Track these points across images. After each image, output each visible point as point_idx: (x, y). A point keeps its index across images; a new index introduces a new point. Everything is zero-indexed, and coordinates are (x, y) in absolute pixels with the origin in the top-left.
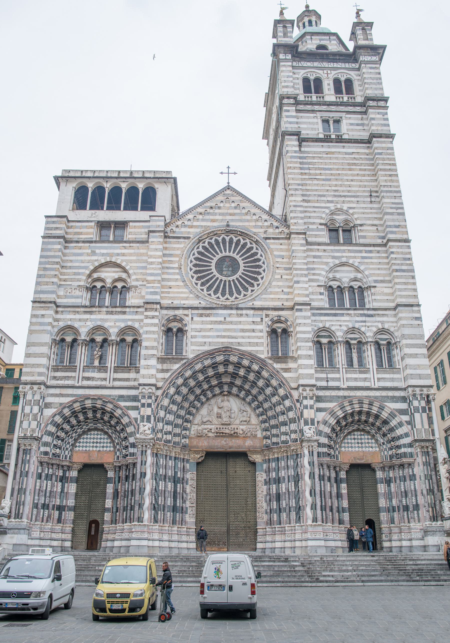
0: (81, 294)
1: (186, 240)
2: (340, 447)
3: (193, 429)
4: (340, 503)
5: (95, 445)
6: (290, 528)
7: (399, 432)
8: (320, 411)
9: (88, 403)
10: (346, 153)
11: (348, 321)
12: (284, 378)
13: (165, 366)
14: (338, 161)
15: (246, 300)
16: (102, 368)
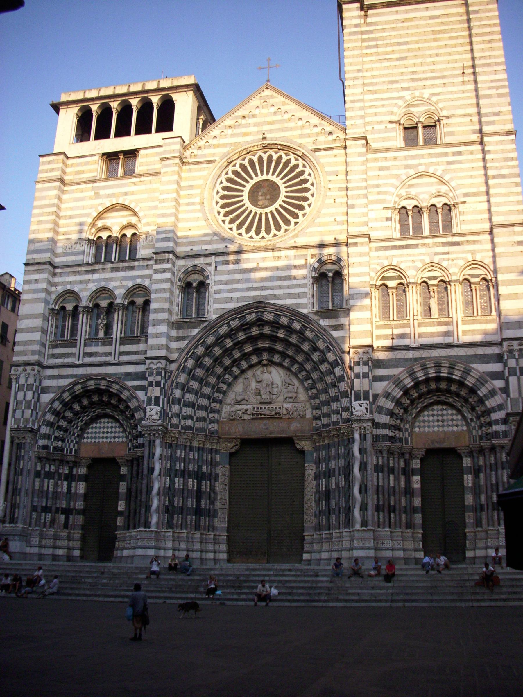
0: (82, 249)
1: (211, 165)
2: (413, 426)
3: (224, 410)
4: (408, 502)
5: (105, 435)
6: (338, 535)
7: (490, 403)
9: (91, 384)
10: (431, 18)
11: (424, 254)
12: (333, 338)
13: (181, 333)
14: (418, 31)
15: (286, 237)
16: (107, 341)
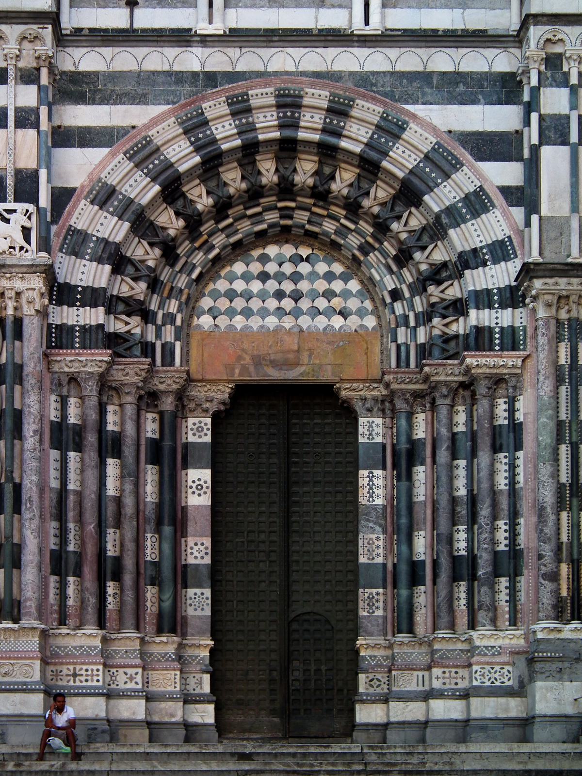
8: (82, 144)
